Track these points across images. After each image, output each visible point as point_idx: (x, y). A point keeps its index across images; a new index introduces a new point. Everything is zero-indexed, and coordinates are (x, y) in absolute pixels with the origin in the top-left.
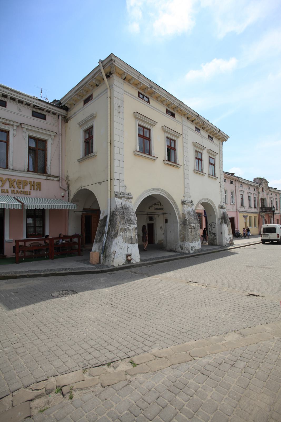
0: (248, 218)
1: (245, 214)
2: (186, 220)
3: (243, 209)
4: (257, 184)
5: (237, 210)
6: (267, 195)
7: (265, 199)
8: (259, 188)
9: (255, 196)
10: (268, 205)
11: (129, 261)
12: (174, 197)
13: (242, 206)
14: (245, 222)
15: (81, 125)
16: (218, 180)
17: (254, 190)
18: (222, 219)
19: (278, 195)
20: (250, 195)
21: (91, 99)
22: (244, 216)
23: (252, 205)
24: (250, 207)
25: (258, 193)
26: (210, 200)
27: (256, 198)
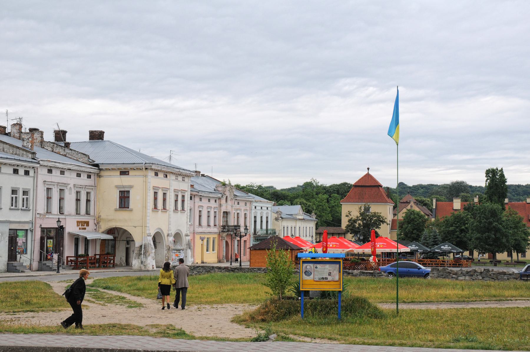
0: (205, 240)
1: (203, 236)
2: (170, 247)
3: (200, 230)
4: (219, 195)
5: (194, 230)
6: (232, 206)
7: (229, 212)
8: (222, 198)
9: (216, 210)
10: (232, 222)
11: (153, 268)
12: (164, 232)
13: (200, 224)
14: (202, 244)
15: (117, 187)
16: (186, 213)
17: (216, 201)
18: (187, 245)
19: (248, 204)
20: (209, 210)
21: (127, 173)
22: (201, 238)
23: (212, 224)
24: (209, 226)
25: (220, 205)
26: (180, 230)
27: (217, 213)
